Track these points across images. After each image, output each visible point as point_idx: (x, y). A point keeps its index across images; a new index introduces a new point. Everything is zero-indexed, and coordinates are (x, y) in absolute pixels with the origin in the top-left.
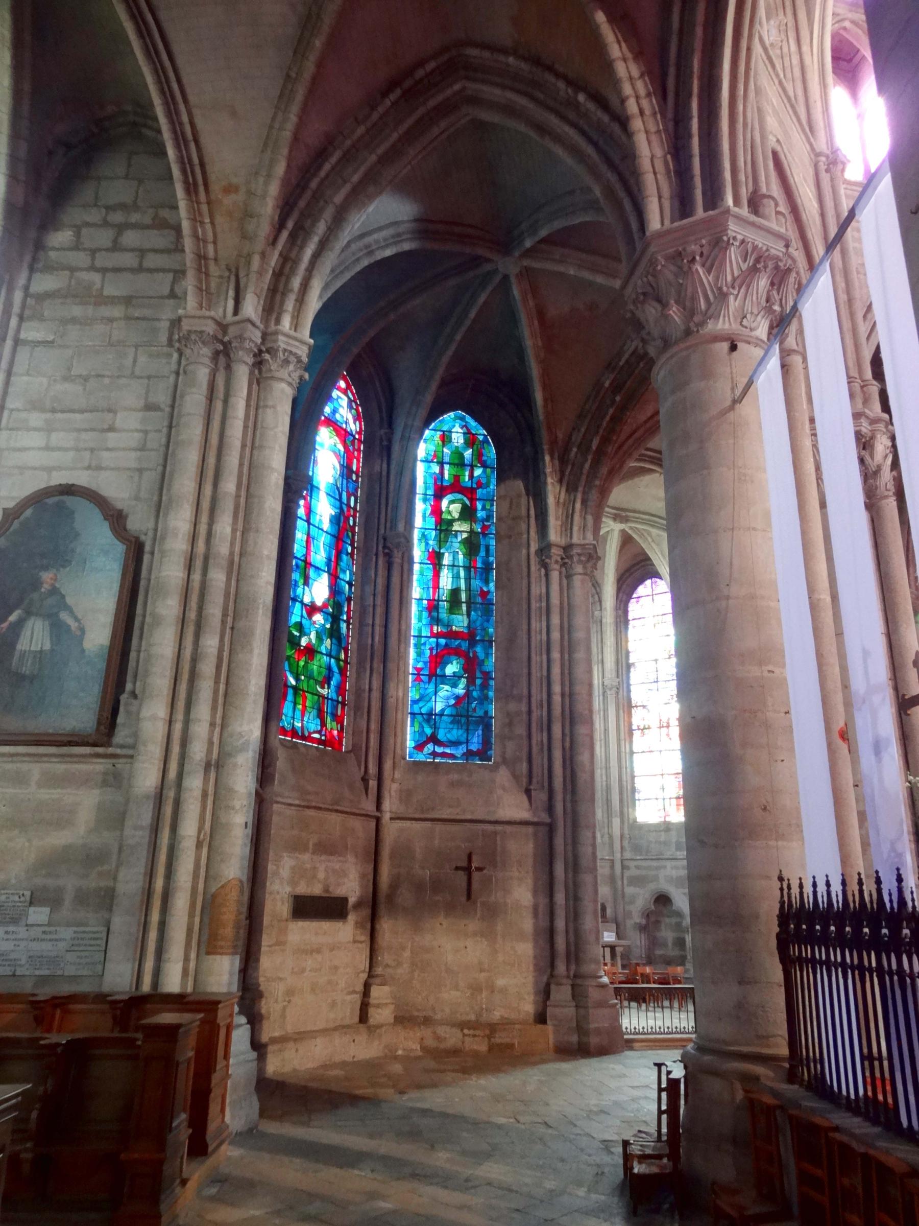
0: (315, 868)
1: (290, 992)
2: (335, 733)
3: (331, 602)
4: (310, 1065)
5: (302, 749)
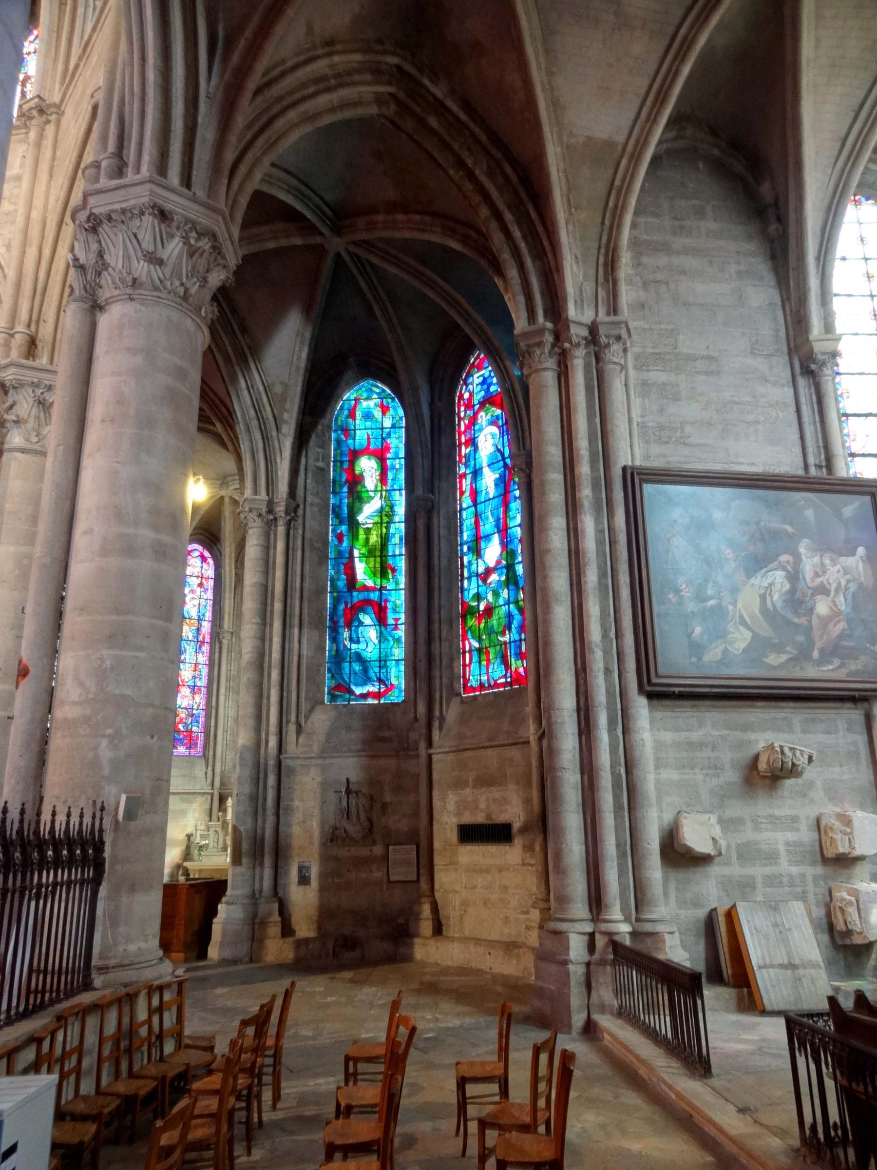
0: (476, 801)
1: (465, 904)
2: (521, 670)
3: (504, 555)
4: (450, 963)
5: (480, 699)
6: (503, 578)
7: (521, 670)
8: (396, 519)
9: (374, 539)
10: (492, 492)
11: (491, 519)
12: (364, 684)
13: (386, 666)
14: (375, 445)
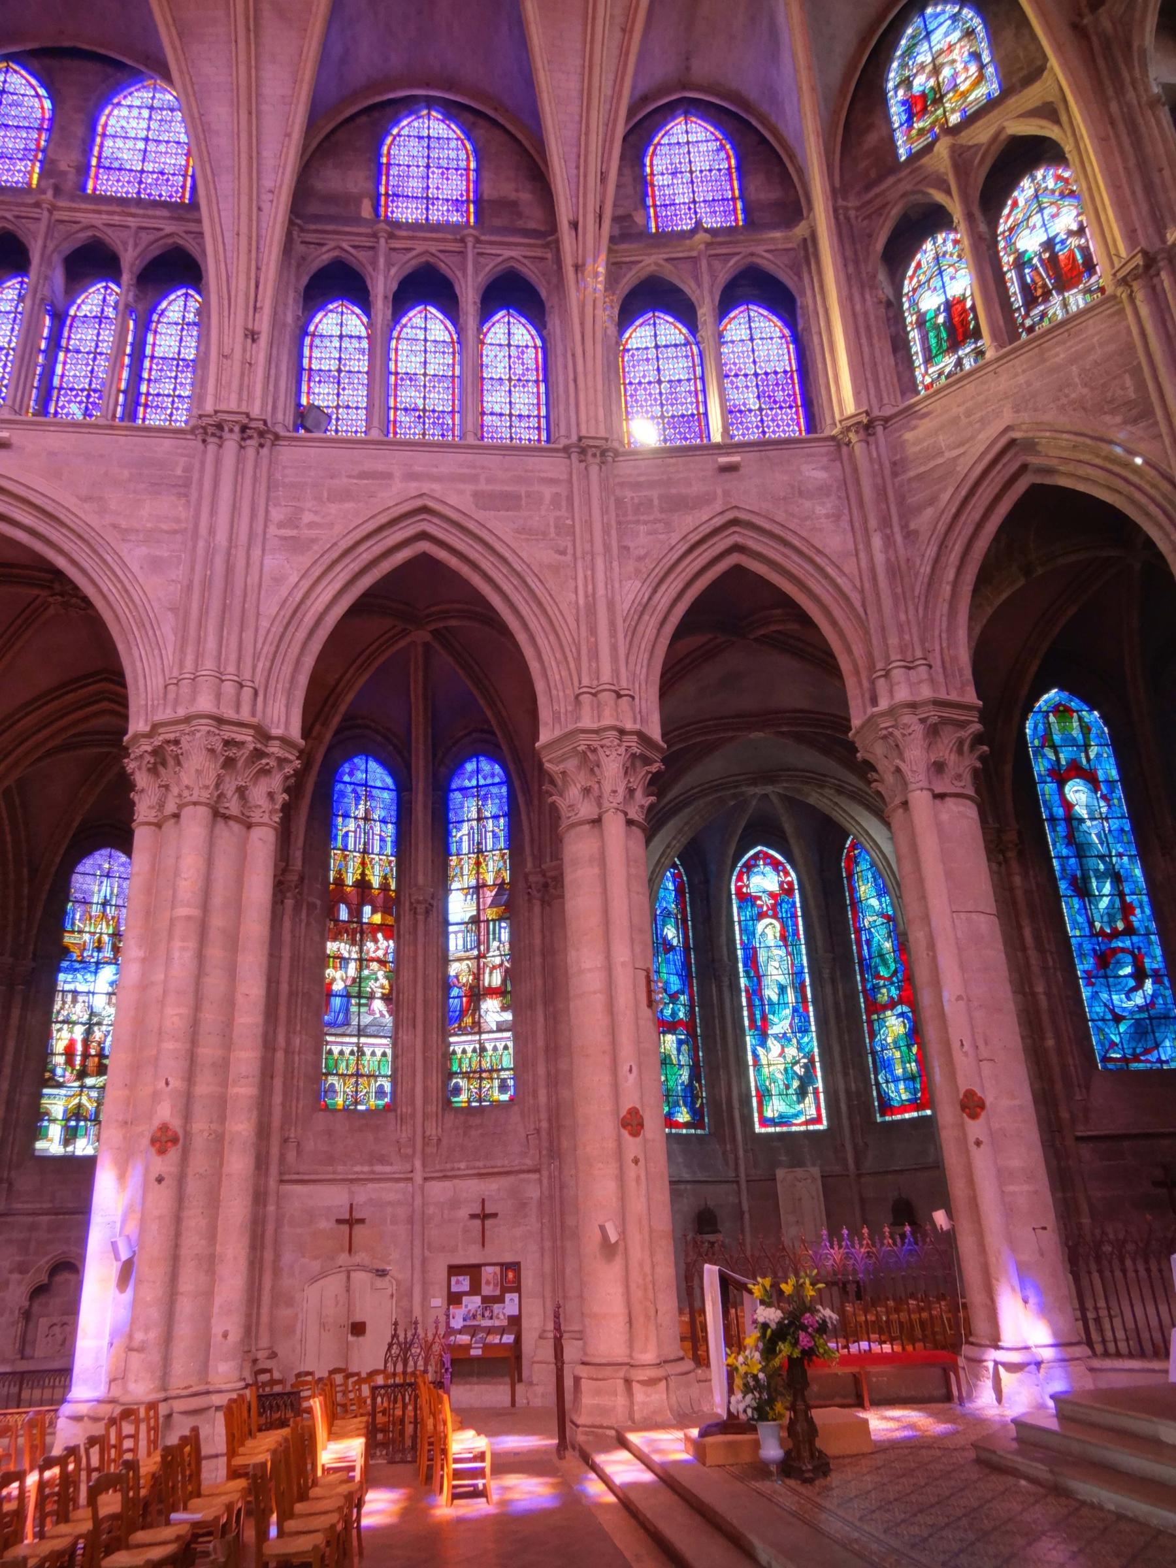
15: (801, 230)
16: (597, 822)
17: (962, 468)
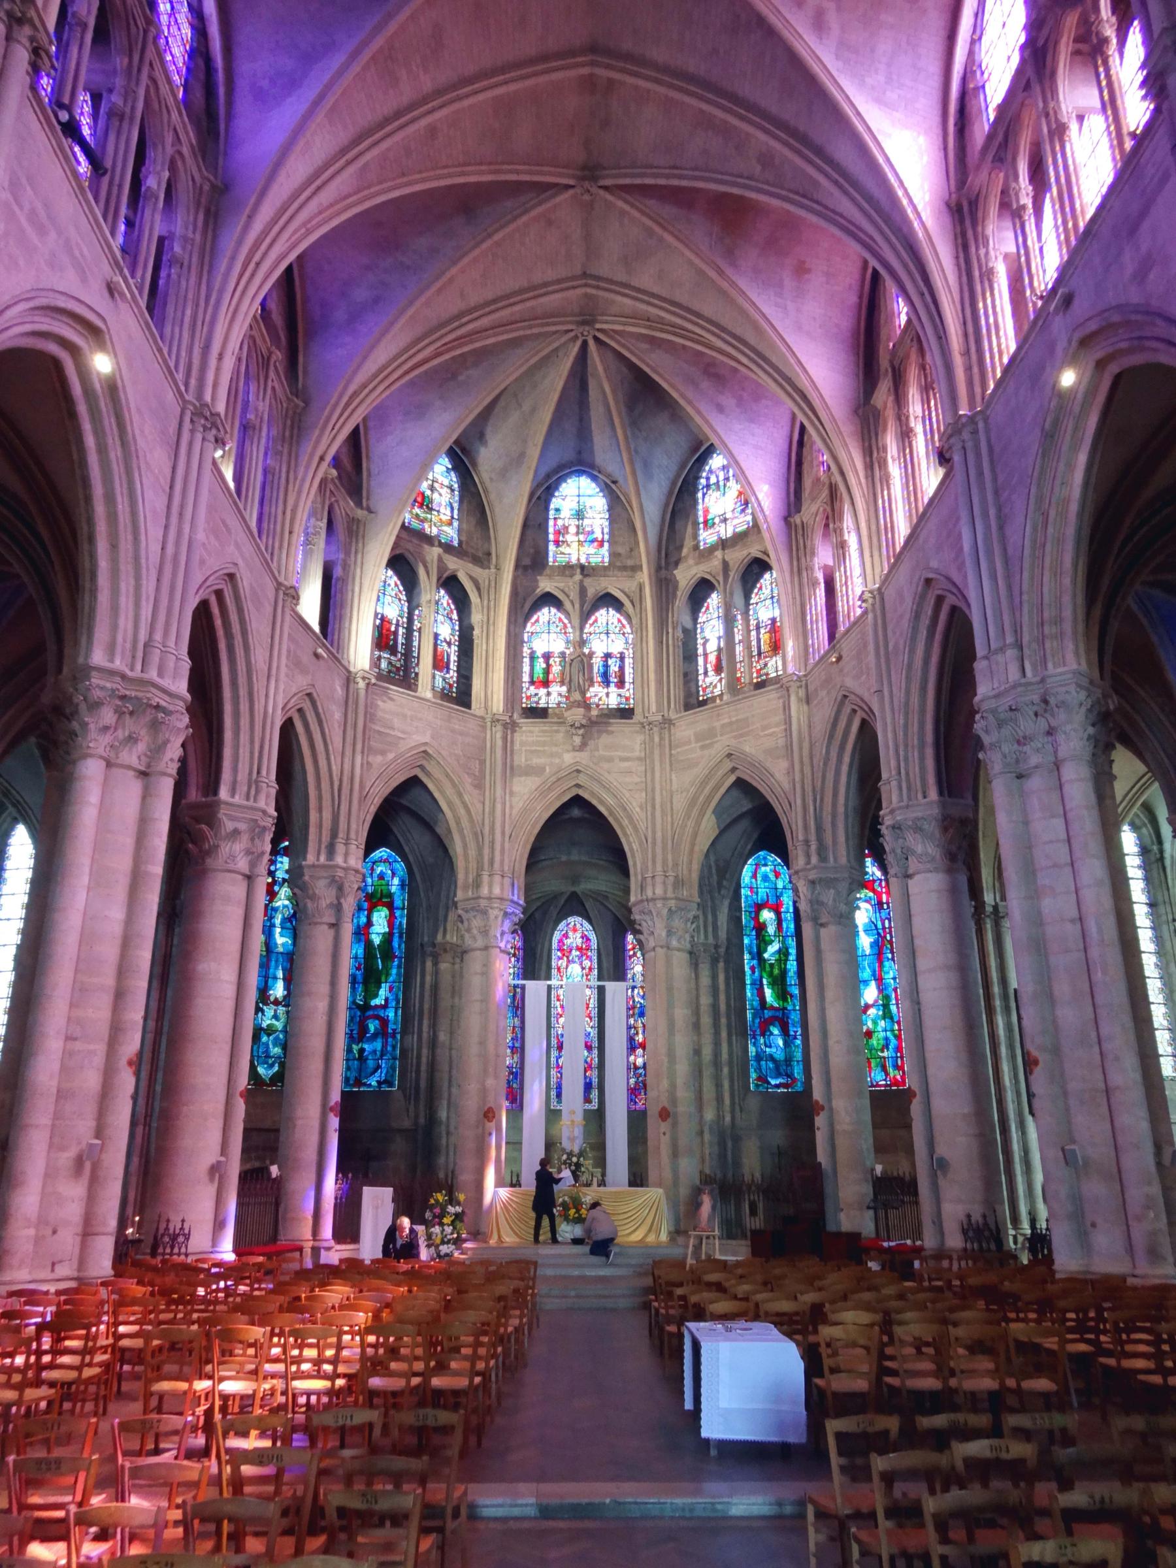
6: (881, 1013)
7: (898, 1077)
8: (791, 958)
9: (776, 971)
10: (868, 952)
11: (868, 970)
12: (776, 1077)
13: (790, 1065)
14: (772, 901)
15: (360, 513)
16: (250, 878)
17: (403, 746)
